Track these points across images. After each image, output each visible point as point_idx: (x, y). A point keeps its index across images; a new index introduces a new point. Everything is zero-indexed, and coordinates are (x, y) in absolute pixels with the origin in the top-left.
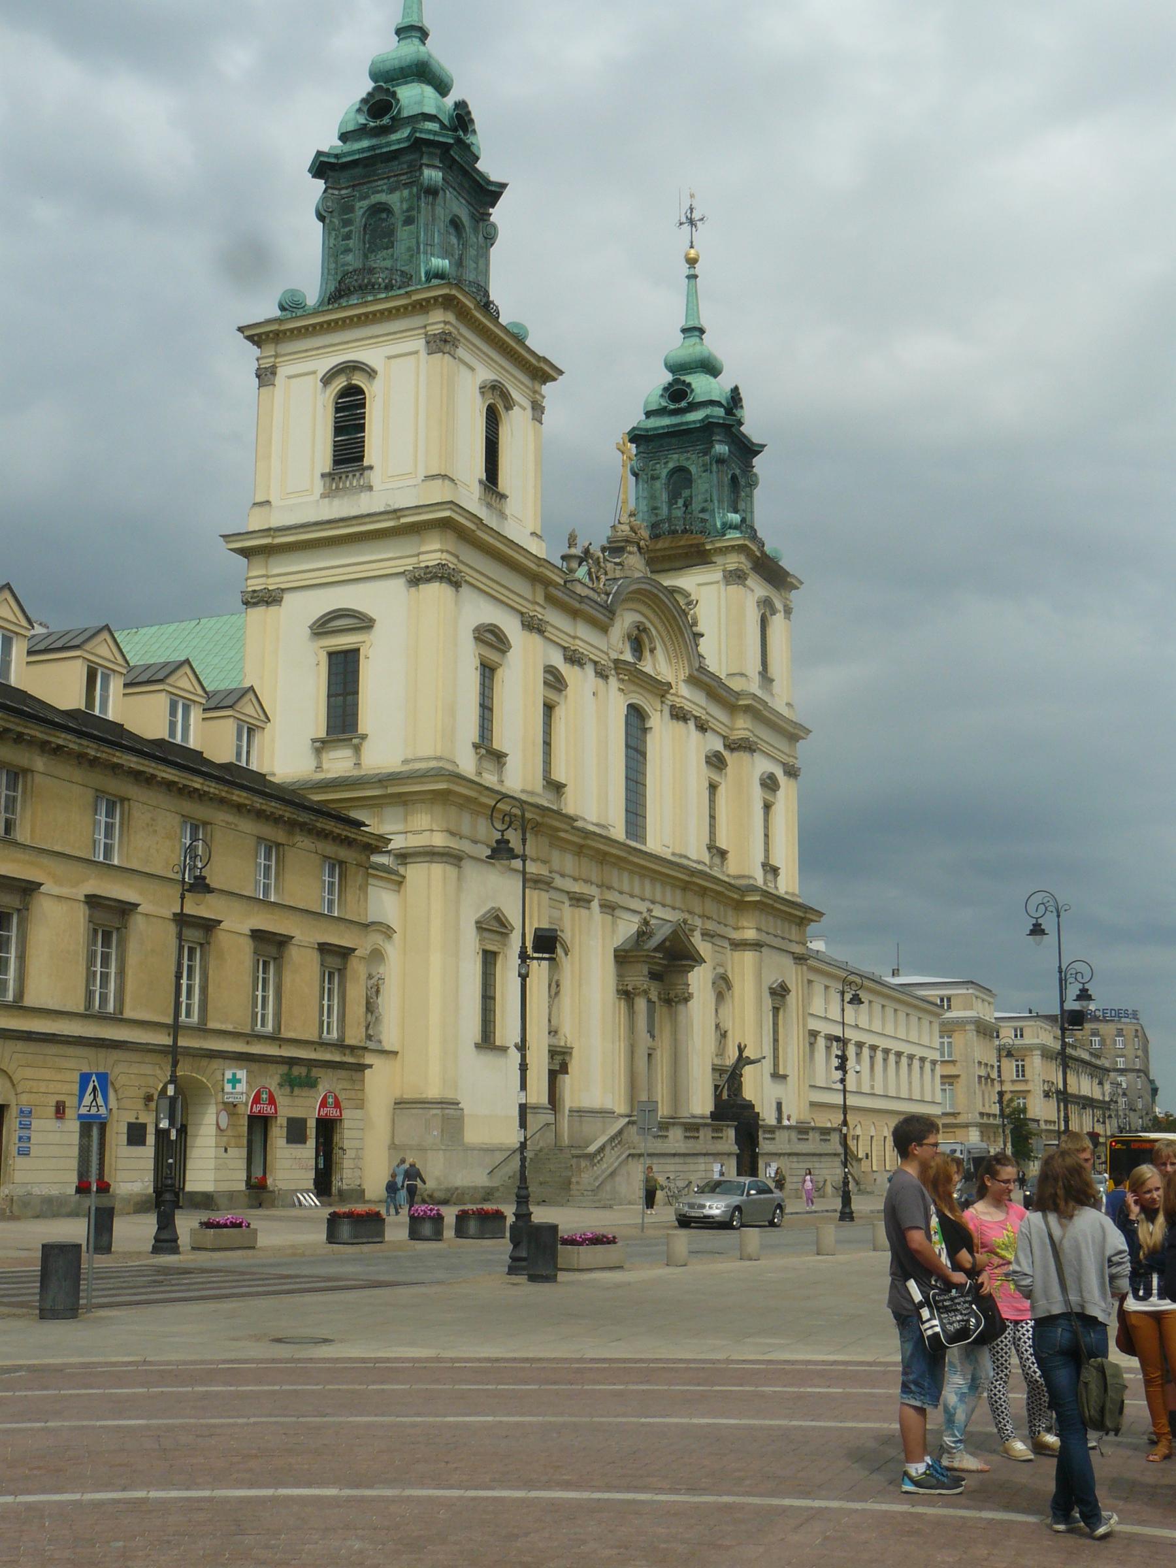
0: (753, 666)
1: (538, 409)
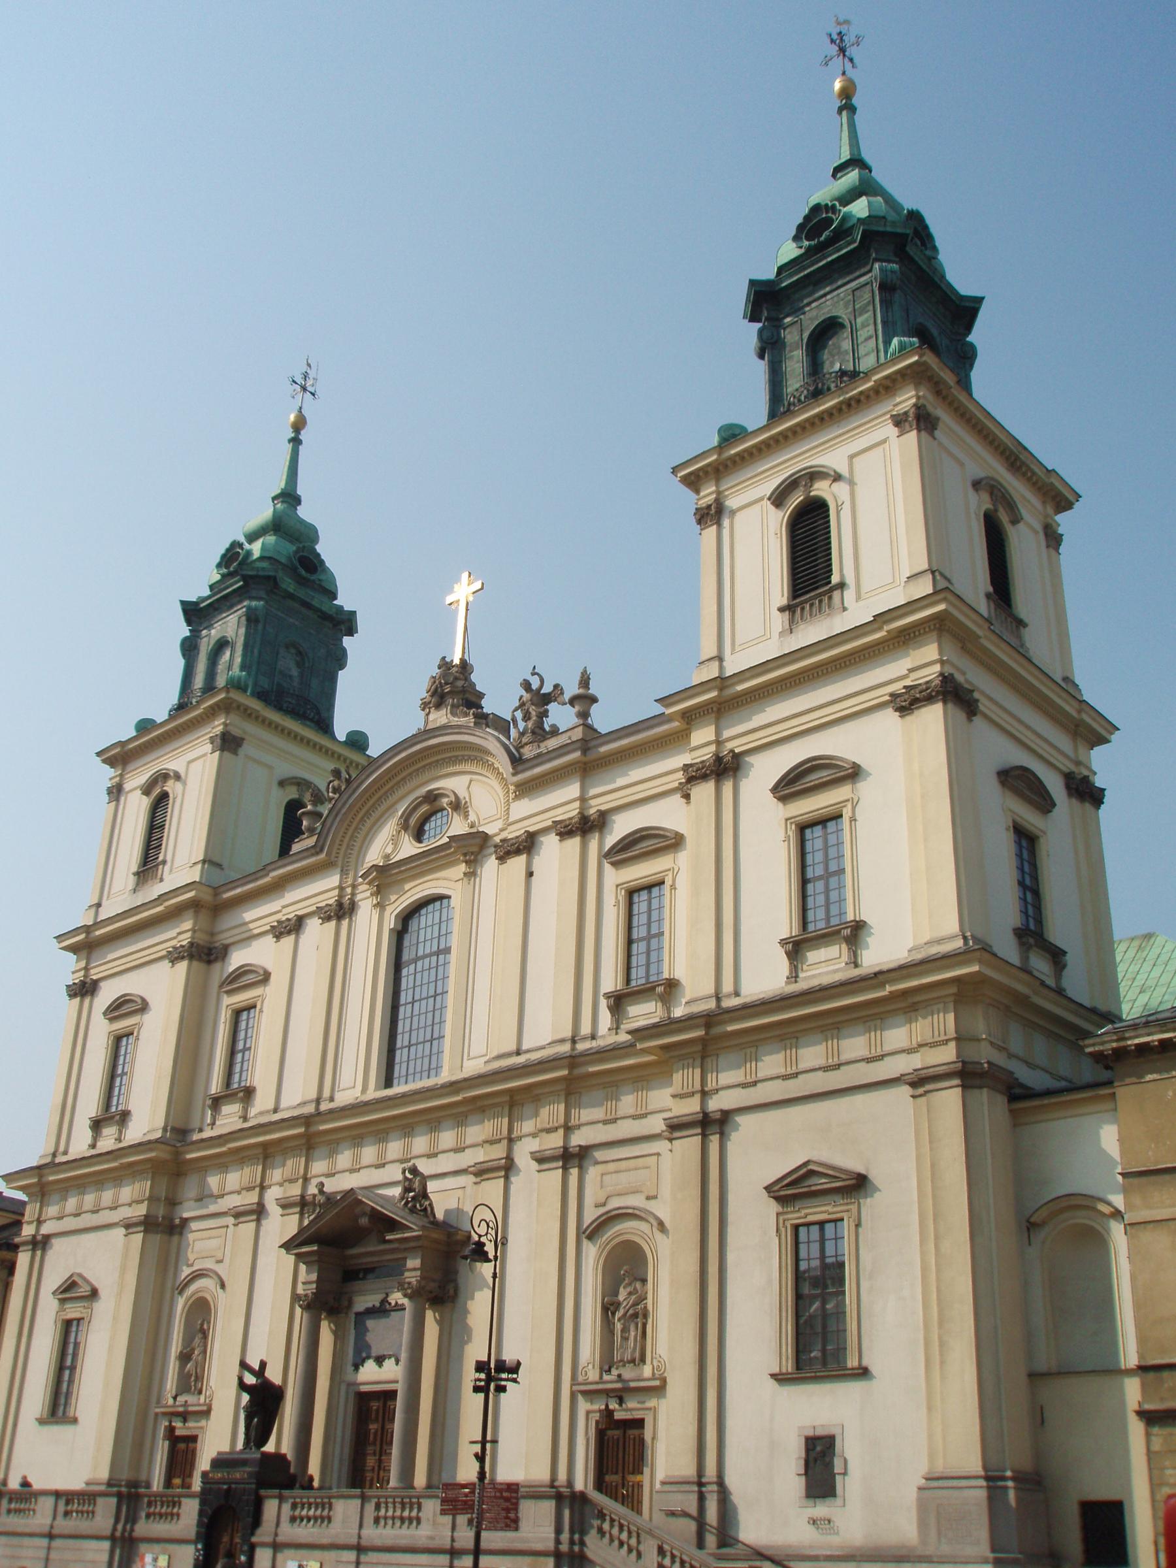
1: (1053, 539)
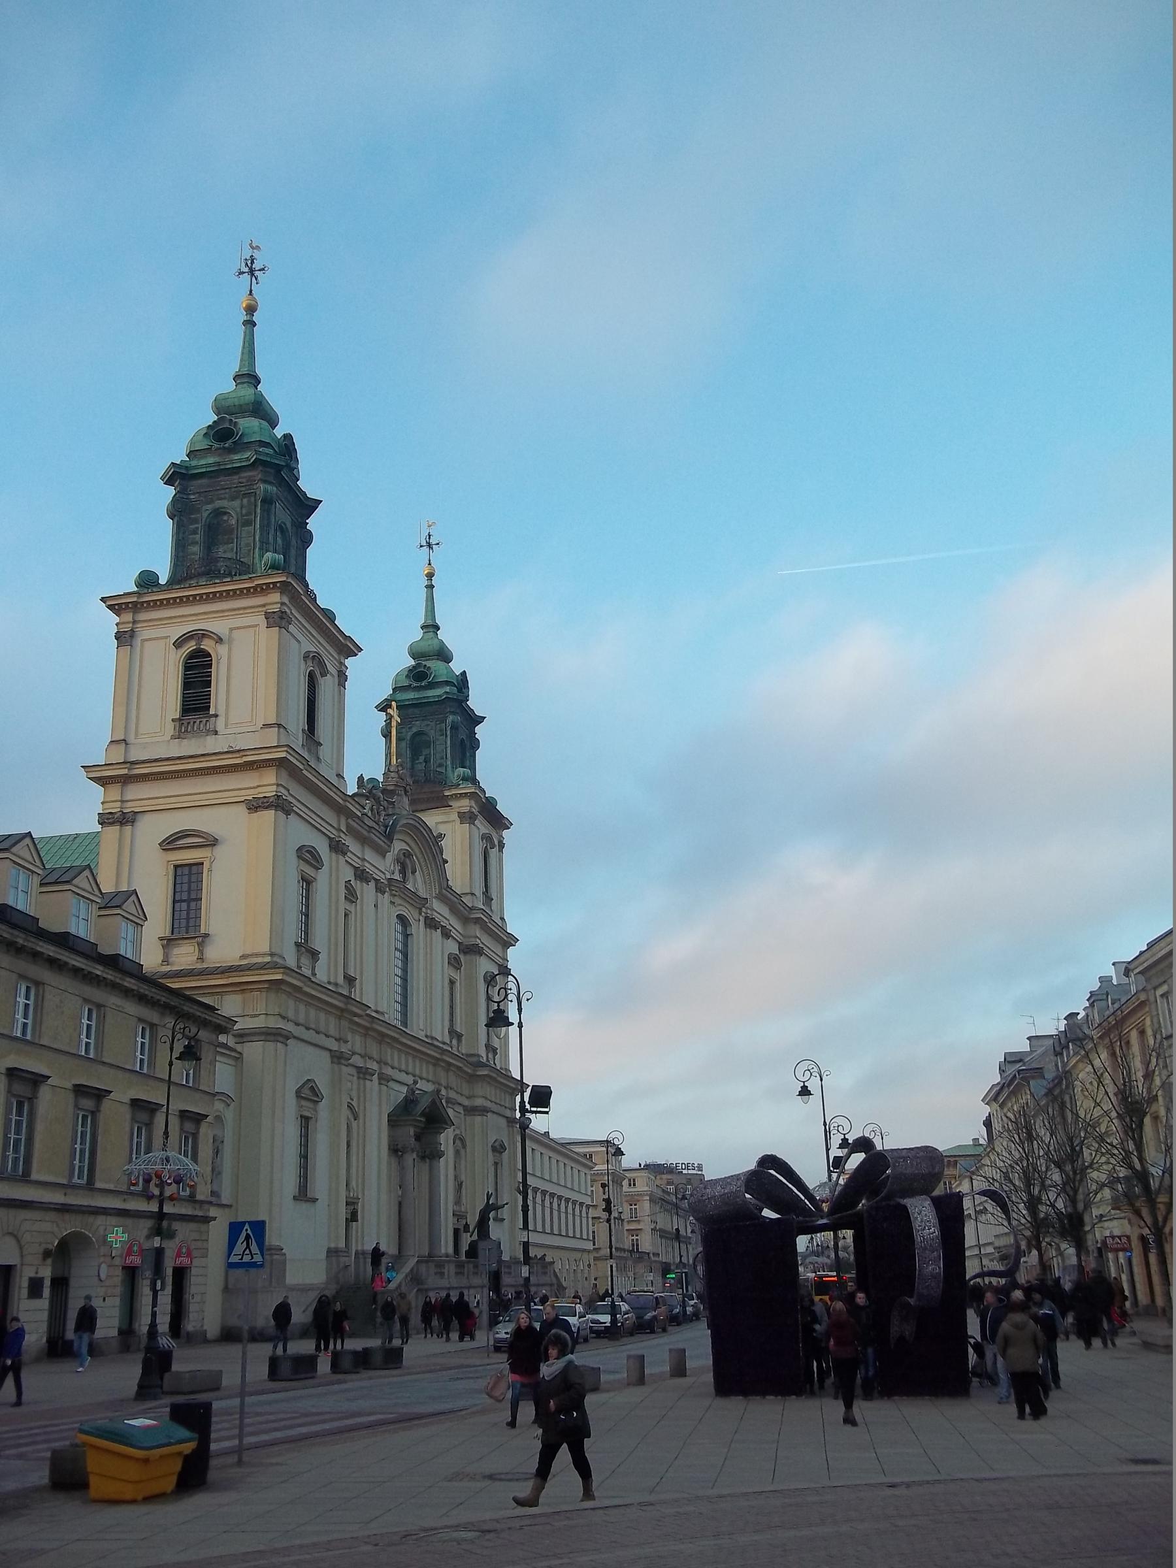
1: (342, 677)
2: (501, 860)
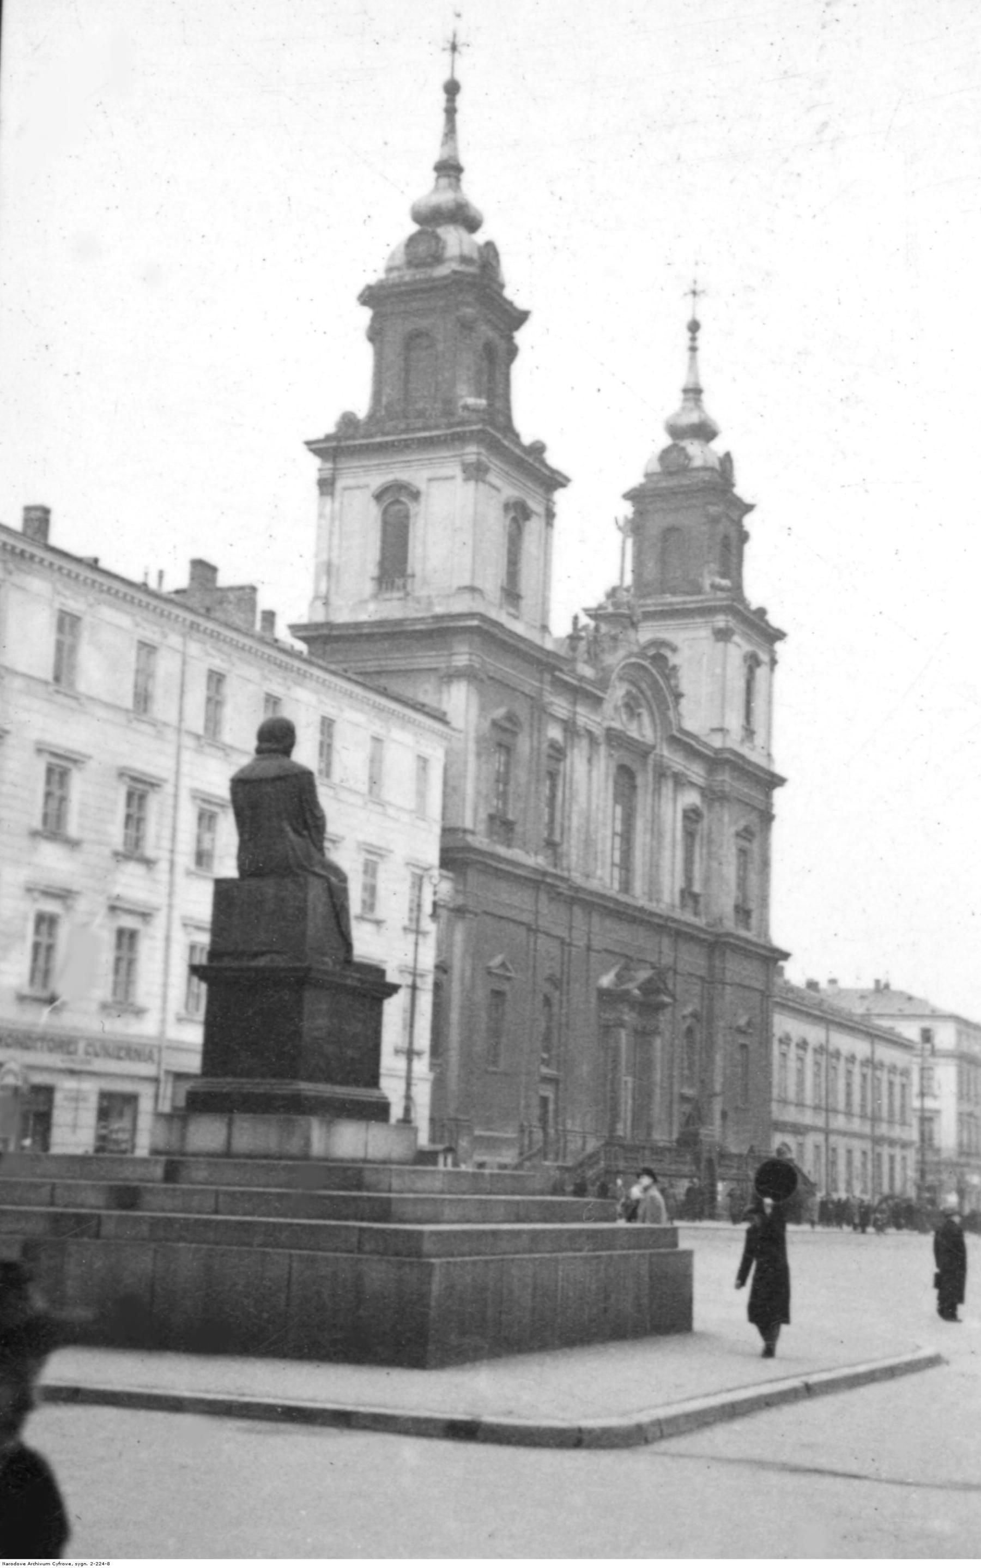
0: (734, 722)
2: (770, 685)
